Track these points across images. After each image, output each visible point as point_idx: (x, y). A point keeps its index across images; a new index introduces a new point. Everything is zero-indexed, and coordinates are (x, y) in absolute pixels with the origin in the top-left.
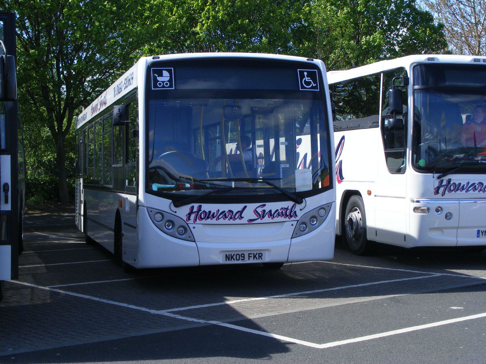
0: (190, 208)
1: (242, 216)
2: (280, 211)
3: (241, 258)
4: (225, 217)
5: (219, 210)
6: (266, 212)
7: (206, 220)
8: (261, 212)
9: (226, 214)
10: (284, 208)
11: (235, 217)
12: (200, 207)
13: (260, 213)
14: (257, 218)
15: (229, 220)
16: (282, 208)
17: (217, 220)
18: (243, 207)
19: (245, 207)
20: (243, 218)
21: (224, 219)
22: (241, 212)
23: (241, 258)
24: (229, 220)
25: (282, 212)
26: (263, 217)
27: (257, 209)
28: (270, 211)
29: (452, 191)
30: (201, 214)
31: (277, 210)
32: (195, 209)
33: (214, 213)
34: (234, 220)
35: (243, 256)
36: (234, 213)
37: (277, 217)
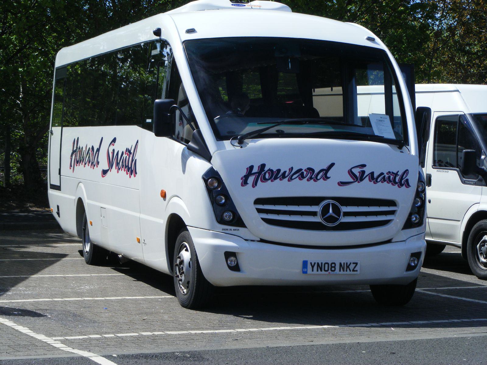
1: (328, 175)
2: (387, 176)
4: (302, 177)
5: (292, 168)
6: (366, 174)
7: (272, 181)
9: (303, 173)
10: (393, 173)
13: (358, 174)
14: (352, 180)
15: (308, 180)
16: (389, 172)
17: (289, 181)
20: (329, 178)
21: (300, 179)
25: (389, 177)
26: (362, 179)
27: (352, 170)
31: (382, 174)
33: (285, 172)
37: (382, 182)
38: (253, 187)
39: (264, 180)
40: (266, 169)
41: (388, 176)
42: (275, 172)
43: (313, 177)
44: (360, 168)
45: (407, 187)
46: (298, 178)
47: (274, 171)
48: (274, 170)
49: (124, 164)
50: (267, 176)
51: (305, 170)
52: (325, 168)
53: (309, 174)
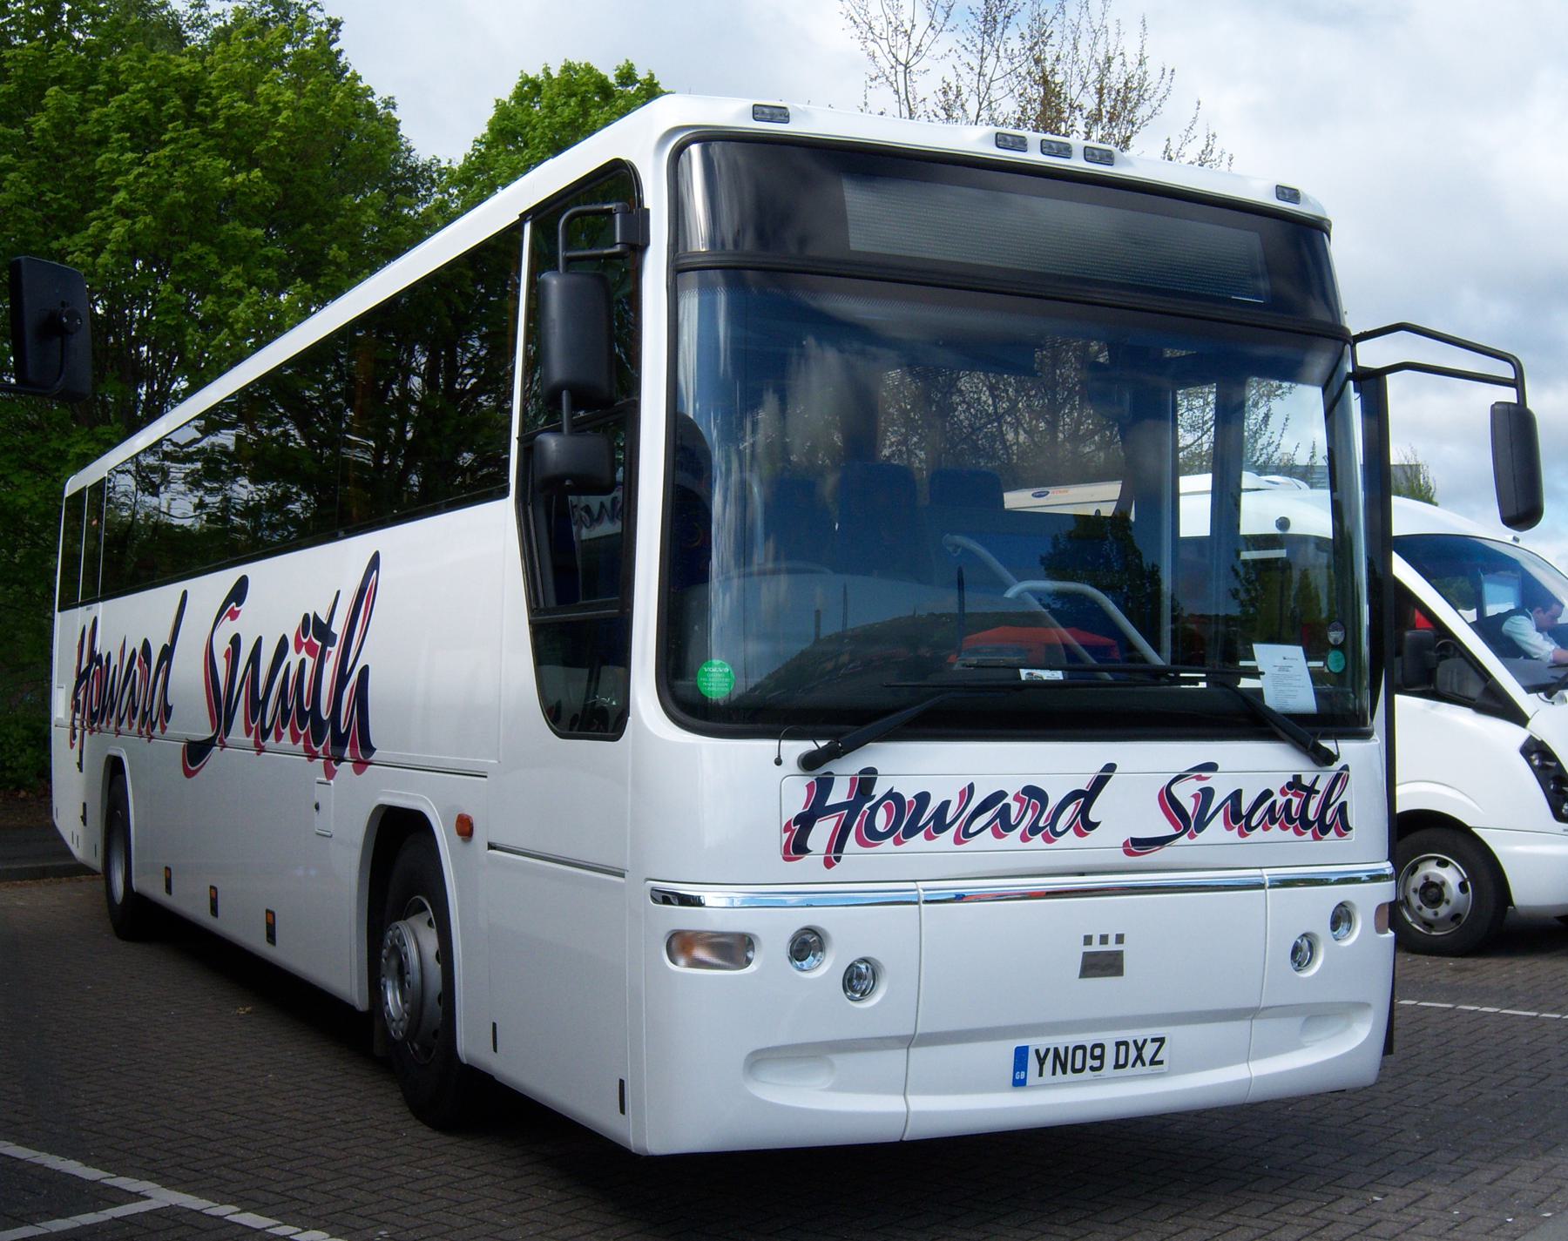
1: (1092, 817)
2: (1281, 800)
3: (1090, 1062)
4: (1004, 824)
5: (971, 787)
7: (898, 842)
8: (1195, 796)
9: (1007, 807)
11: (1053, 824)
13: (1189, 806)
14: (1173, 832)
15: (1024, 838)
17: (957, 841)
18: (1096, 768)
19: (1111, 768)
20: (1092, 826)
21: (998, 835)
22: (1085, 798)
23: (1090, 1062)
24: (1024, 838)
25: (1289, 802)
26: (1201, 825)
27: (1174, 789)
28: (1237, 795)
31: (1267, 794)
33: (945, 805)
34: (1048, 840)
35: (1097, 1052)
36: (1054, 801)
37: (1266, 828)
38: (829, 863)
39: (872, 836)
40: (879, 791)
41: (1284, 799)
42: (911, 803)
43: (1041, 824)
44: (1199, 778)
45: (1340, 834)
47: (907, 799)
48: (908, 797)
49: (292, 704)
50: (881, 822)
51: (1017, 798)
52: (1084, 788)
53: (1030, 811)
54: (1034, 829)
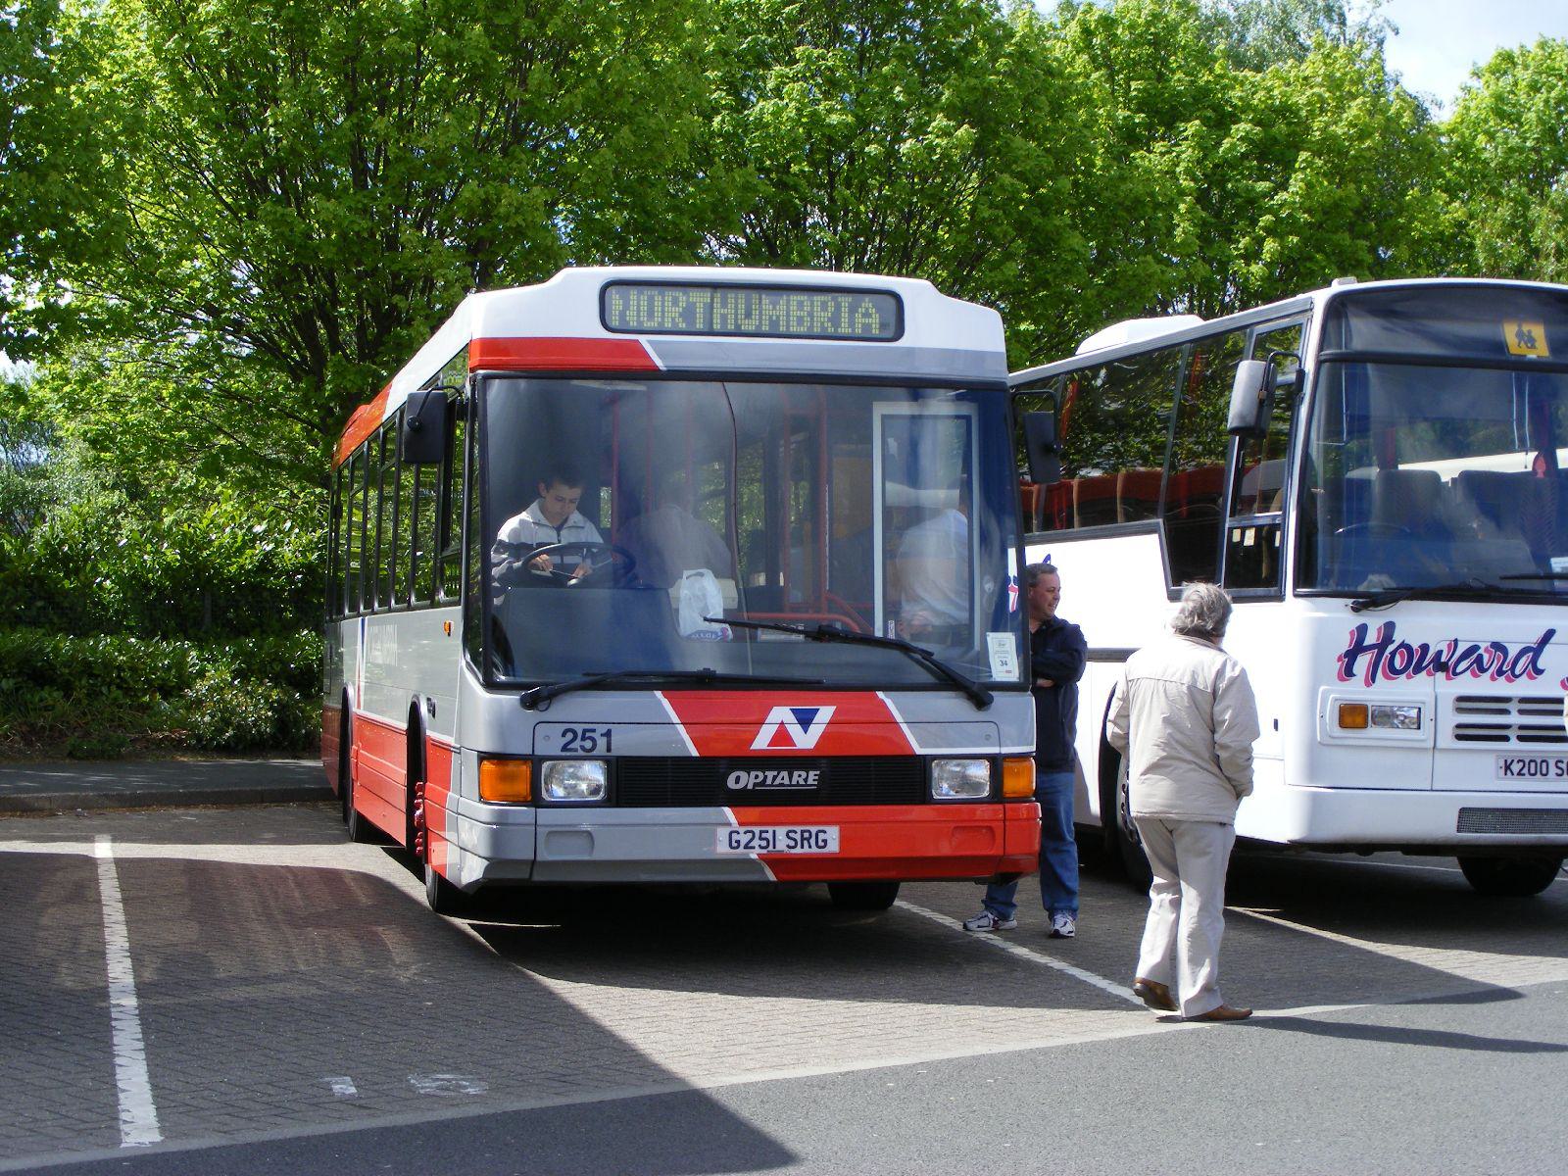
0: (1352, 633)
1: (1540, 665)
4: (1480, 667)
7: (1409, 677)
9: (1480, 657)
12: (1390, 627)
15: (1493, 678)
20: (1540, 672)
21: (1475, 675)
29: (1399, 672)
30: (1393, 654)
32: (1371, 639)
33: (1440, 653)
34: (1509, 680)
36: (1513, 652)
39: (1393, 672)
46: (1468, 672)
50: (1398, 663)
51: (1486, 650)
54: (1500, 672)
